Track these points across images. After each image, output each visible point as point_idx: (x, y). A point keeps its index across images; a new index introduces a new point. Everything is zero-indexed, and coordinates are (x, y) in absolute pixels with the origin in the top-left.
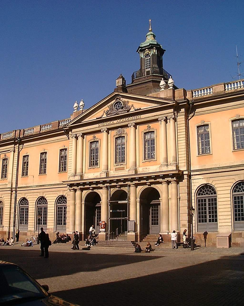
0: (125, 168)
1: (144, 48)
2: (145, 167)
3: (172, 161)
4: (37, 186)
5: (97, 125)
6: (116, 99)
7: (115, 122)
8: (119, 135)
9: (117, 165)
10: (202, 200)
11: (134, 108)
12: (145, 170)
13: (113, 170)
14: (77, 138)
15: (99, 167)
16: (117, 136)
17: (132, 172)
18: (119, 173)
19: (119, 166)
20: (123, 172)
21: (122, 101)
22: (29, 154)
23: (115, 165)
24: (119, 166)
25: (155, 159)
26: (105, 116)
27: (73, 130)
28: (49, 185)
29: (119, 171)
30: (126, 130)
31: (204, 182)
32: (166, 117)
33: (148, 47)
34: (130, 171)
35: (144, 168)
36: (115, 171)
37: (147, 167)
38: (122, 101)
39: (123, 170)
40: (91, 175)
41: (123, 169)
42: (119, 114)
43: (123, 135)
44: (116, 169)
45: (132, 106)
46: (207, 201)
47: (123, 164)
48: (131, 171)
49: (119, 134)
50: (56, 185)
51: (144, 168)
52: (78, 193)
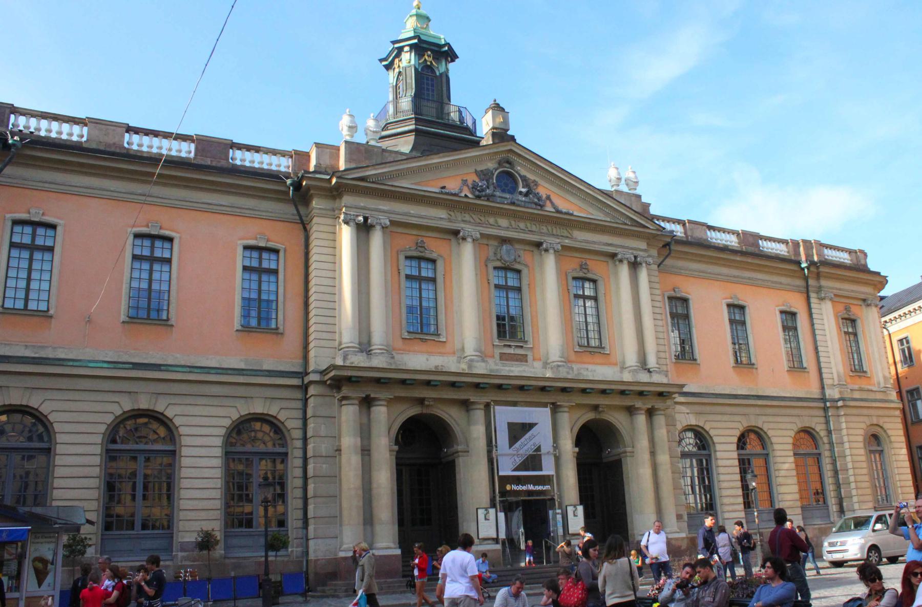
0: (530, 358)
1: (425, 46)
4: (115, 364)
5: (442, 213)
7: (503, 222)
9: (505, 346)
12: (585, 373)
13: (493, 357)
14: (364, 229)
15: (444, 340)
16: (498, 264)
17: (568, 373)
18: (512, 369)
19: (511, 351)
21: (520, 175)
22: (62, 222)
23: (497, 342)
24: (511, 351)
26: (466, 191)
27: (347, 199)
28: (188, 369)
30: (527, 256)
31: (693, 421)
32: (636, 257)
33: (436, 49)
34: (560, 369)
37: (590, 367)
38: (520, 175)
40: (419, 360)
41: (523, 359)
42: (518, 206)
43: (517, 267)
44: (503, 357)
45: (548, 198)
47: (522, 347)
50: (230, 372)
52: (380, 412)
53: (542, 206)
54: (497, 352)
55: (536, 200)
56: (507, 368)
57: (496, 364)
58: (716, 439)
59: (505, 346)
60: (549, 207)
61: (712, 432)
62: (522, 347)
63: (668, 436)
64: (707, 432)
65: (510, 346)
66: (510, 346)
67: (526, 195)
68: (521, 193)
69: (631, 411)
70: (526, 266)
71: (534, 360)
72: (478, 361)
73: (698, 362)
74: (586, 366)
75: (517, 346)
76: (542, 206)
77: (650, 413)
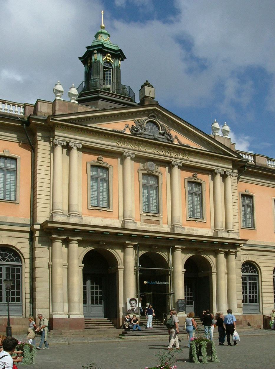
0: (161, 222)
2: (191, 228)
3: (221, 227)
6: (151, 116)
8: (150, 171)
9: (147, 215)
10: (253, 278)
11: (178, 141)
16: (146, 172)
18: (150, 227)
19: (150, 218)
20: (159, 228)
21: (159, 123)
24: (150, 218)
25: (204, 221)
29: (151, 225)
35: (190, 229)
36: (143, 223)
37: (195, 228)
38: (159, 123)
39: (156, 224)
41: (157, 223)
43: (155, 174)
44: (145, 221)
46: (248, 279)
47: (156, 216)
48: (180, 229)
49: (150, 169)
51: (189, 228)
53: (172, 141)
54: (143, 218)
55: (169, 138)
56: (148, 227)
57: (141, 225)
58: (262, 268)
59: (147, 215)
60: (176, 142)
61: (260, 265)
62: (156, 216)
63: (236, 266)
64: (257, 265)
65: (149, 216)
66: (149, 216)
67: (163, 134)
68: (160, 133)
69: (216, 253)
70: (160, 173)
71: (163, 223)
72: (131, 223)
73: (255, 229)
74: (193, 228)
75: (154, 216)
76: (172, 141)
77: (227, 254)
